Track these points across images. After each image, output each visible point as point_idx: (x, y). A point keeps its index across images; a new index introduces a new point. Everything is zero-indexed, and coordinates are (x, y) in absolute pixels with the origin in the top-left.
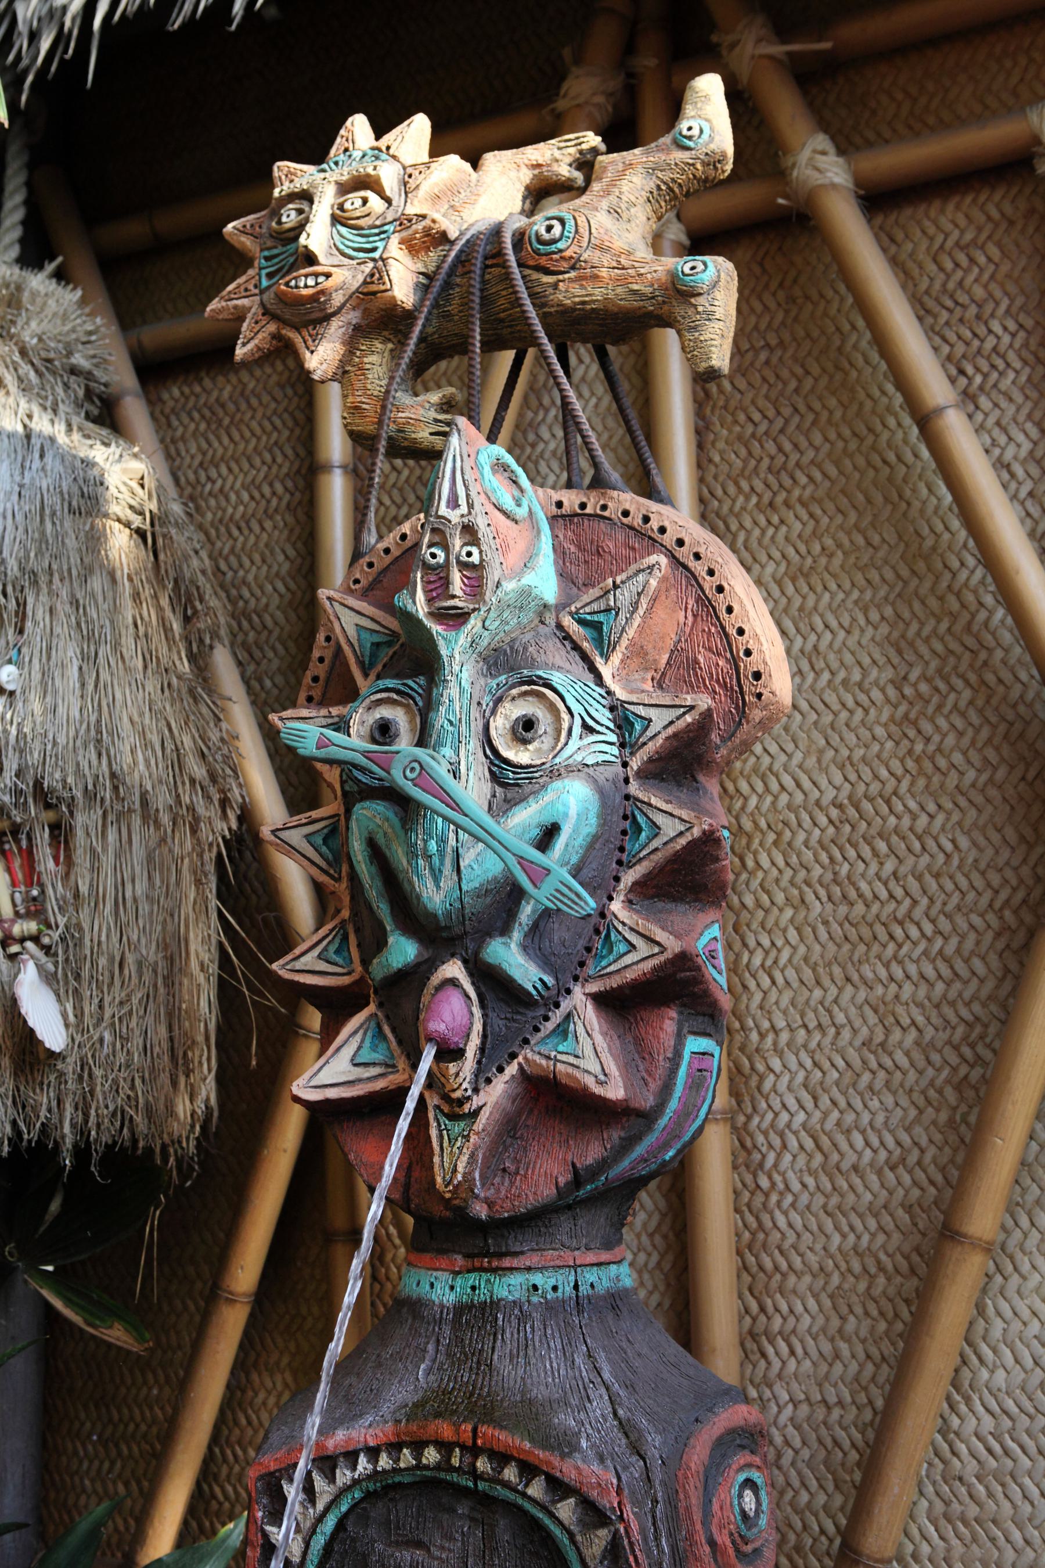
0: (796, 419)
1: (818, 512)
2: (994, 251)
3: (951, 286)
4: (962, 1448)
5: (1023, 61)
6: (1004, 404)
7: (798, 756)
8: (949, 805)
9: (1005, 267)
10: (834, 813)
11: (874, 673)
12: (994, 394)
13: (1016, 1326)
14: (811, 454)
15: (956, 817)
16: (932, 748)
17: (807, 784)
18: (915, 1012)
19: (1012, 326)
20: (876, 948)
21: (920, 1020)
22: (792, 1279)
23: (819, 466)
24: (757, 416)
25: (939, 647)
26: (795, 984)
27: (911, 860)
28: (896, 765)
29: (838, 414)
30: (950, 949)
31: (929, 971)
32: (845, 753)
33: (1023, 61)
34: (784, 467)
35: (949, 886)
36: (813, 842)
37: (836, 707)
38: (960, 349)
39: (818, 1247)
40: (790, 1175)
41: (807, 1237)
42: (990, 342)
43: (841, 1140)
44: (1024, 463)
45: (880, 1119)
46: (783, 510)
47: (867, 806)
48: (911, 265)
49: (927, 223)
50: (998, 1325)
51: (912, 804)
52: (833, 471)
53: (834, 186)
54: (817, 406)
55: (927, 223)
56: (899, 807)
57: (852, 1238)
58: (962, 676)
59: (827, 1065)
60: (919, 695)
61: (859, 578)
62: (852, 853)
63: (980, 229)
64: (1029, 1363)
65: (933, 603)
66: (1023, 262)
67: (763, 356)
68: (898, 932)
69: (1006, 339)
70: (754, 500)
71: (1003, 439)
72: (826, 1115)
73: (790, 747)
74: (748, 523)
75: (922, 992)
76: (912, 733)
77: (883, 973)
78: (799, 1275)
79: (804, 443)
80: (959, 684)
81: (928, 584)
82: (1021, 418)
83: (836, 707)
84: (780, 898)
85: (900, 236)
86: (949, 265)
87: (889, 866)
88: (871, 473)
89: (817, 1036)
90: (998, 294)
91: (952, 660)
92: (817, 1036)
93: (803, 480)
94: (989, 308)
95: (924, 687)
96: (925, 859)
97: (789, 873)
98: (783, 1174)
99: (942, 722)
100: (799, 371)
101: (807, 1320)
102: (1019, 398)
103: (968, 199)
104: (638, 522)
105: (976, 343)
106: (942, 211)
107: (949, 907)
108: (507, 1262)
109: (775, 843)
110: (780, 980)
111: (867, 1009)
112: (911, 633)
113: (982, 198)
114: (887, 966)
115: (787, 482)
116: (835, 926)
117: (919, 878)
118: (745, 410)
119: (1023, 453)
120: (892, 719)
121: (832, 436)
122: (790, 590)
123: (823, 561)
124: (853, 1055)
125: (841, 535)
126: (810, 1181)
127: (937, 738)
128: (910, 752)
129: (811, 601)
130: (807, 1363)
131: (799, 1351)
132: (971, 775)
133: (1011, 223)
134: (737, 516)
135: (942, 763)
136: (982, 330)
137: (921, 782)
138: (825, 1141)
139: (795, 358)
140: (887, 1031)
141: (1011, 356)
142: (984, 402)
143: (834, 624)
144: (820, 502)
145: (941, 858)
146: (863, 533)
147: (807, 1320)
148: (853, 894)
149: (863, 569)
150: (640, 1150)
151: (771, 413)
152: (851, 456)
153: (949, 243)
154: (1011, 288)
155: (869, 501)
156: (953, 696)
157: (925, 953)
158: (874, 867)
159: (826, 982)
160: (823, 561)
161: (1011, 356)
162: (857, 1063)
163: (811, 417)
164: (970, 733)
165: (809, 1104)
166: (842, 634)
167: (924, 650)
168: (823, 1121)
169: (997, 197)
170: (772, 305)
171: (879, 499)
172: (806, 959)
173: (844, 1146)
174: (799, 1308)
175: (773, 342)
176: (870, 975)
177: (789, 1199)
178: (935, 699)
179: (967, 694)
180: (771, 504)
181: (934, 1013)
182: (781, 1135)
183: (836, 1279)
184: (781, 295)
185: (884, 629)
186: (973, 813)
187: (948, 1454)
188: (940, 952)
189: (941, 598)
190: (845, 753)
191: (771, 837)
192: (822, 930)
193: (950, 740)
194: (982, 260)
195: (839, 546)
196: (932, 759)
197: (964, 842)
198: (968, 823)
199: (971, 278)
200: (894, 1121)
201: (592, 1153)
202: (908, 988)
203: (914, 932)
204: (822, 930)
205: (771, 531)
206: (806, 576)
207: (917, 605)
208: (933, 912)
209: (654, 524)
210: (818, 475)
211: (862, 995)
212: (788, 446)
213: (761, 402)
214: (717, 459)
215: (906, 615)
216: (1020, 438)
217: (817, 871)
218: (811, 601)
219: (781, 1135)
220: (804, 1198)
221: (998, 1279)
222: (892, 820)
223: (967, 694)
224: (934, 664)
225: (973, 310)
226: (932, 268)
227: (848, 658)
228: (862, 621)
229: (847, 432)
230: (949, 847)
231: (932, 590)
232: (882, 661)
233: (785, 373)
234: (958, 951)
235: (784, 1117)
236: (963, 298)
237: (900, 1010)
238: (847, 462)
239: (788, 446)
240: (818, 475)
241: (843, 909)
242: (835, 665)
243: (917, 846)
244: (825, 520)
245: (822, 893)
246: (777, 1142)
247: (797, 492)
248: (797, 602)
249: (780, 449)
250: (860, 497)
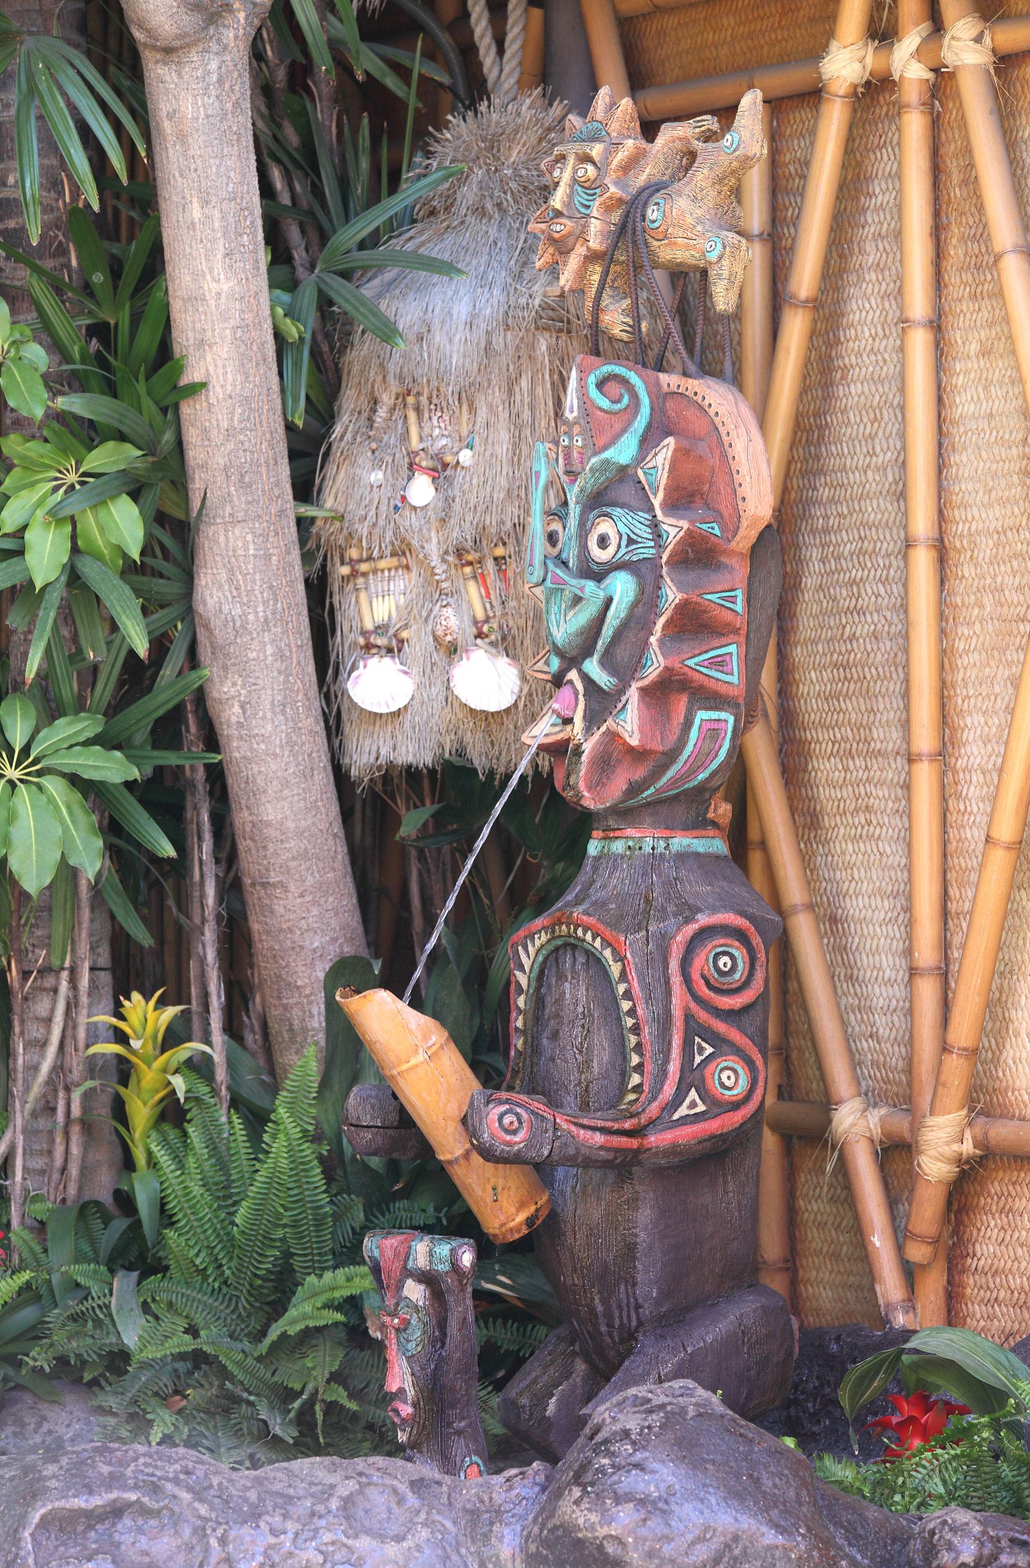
104: (700, 400)
108: (617, 834)
148: (1003, 600)
150: (670, 773)
168: (987, 762)
201: (639, 773)
209: (706, 402)
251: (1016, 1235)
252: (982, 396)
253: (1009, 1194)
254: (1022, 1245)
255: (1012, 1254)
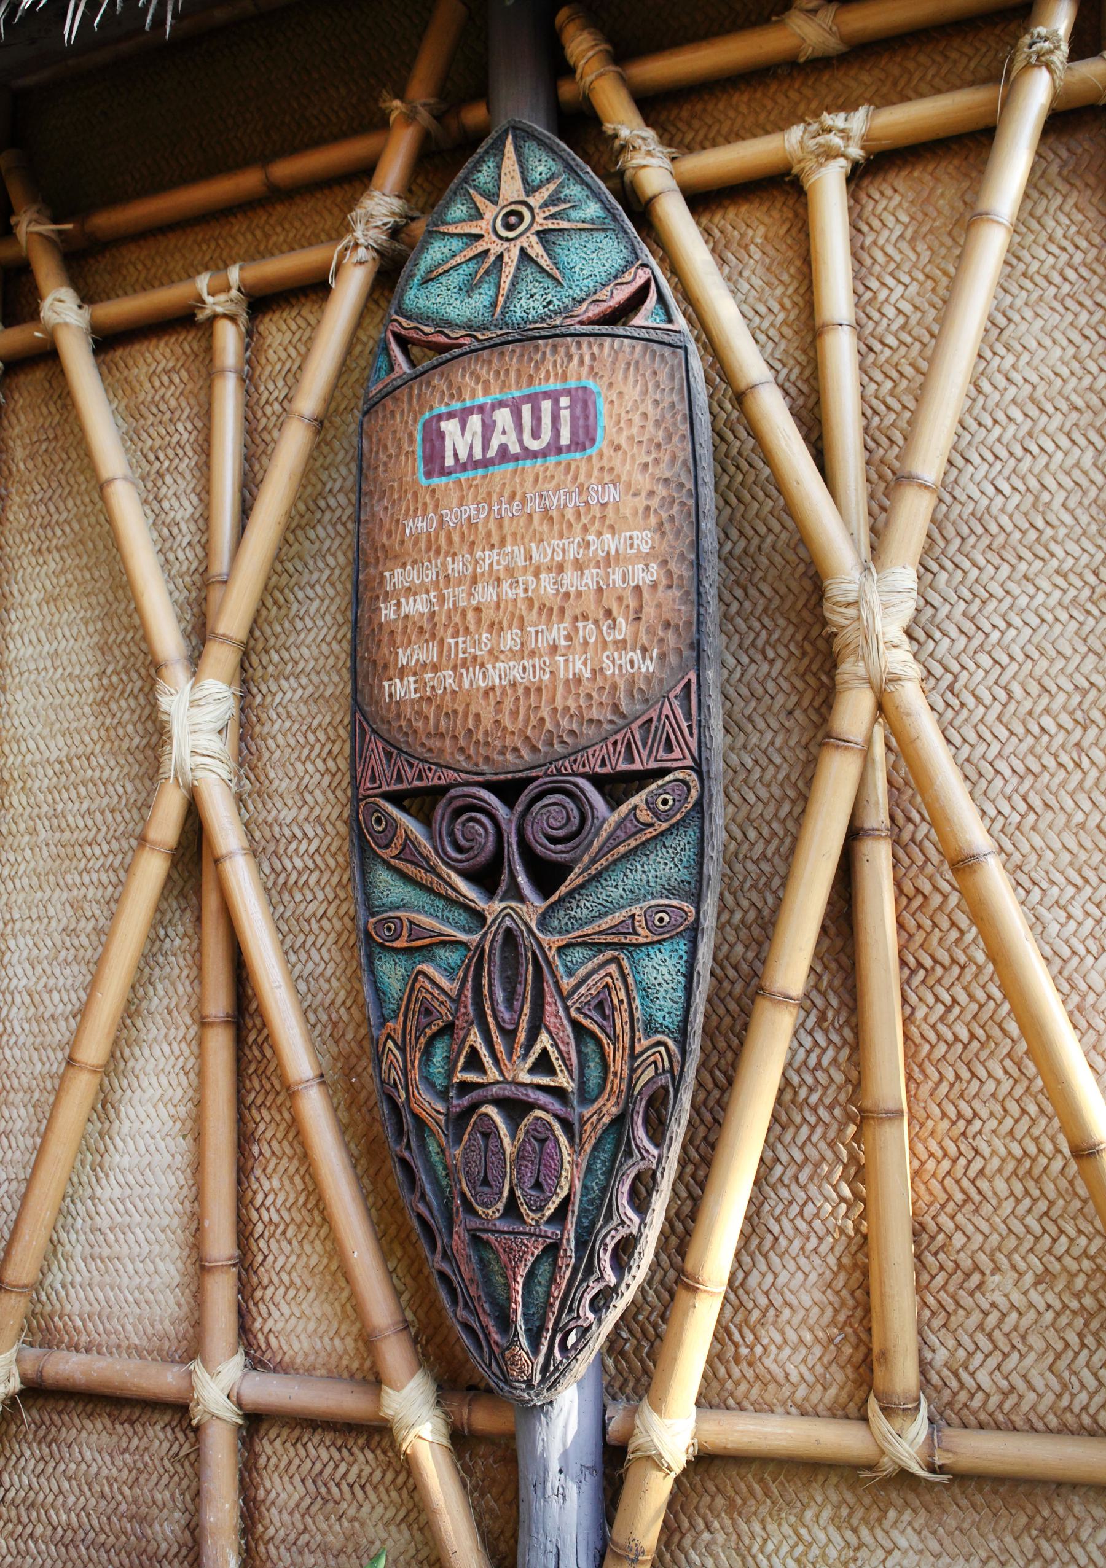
0: (60, 490)
1: (65, 555)
2: (184, 374)
3: (157, 398)
4: (102, 1209)
5: (213, 245)
6: (180, 481)
7: (39, 727)
8: (123, 762)
9: (190, 386)
10: (57, 767)
11: (88, 667)
12: (175, 474)
13: (137, 1124)
14: (65, 515)
15: (126, 770)
16: (116, 721)
17: (42, 747)
18: (95, 906)
19: (190, 427)
20: (75, 861)
21: (97, 912)
22: (12, 1094)
23: (69, 524)
24: (37, 488)
25: (126, 650)
26: (27, 888)
27: (98, 800)
28: (94, 733)
29: (83, 487)
30: (116, 864)
31: (105, 880)
32: (66, 725)
33: (213, 245)
34: (49, 524)
35: (119, 819)
36: (44, 789)
37: (64, 692)
38: (158, 442)
39: (28, 1072)
40: (16, 1023)
41: (22, 1064)
42: (176, 437)
43: (45, 996)
44: (187, 521)
45: (69, 982)
46: (46, 553)
47: (76, 762)
48: (135, 383)
49: (147, 355)
50: (127, 1123)
51: (102, 761)
52: (76, 527)
53: (66, 324)
54: (72, 481)
55: (147, 355)
56: (94, 763)
57: (48, 1065)
58: (137, 671)
59: (41, 945)
60: (111, 684)
61: (85, 602)
62: (65, 795)
63: (178, 360)
64: (143, 1150)
65: (125, 619)
66: (201, 383)
67: (44, 446)
68: (88, 851)
69: (186, 435)
70: (30, 547)
71: (176, 505)
72: (39, 979)
73: (35, 721)
74: (25, 564)
75: (99, 894)
76: (105, 711)
77: (78, 880)
78: (16, 1091)
79: (62, 507)
80: (134, 676)
81: (123, 606)
82: (189, 491)
83: (64, 692)
84: (22, 827)
85: (131, 363)
86: (157, 384)
87: (85, 806)
88: (98, 528)
89: (37, 924)
90: (184, 404)
91: (132, 659)
92: (37, 924)
93: (59, 533)
94: (177, 414)
95: (115, 679)
96: (106, 800)
97: (29, 809)
98: (11, 1022)
99: (123, 703)
100: (64, 456)
101: (19, 1123)
102: (189, 477)
103: (173, 340)
105: (168, 438)
106: (157, 347)
107: (118, 834)
109: (22, 788)
110: (18, 886)
111: (67, 905)
112: (110, 641)
113: (181, 338)
114: (80, 874)
115: (50, 534)
116: (52, 847)
117: (102, 813)
118: (30, 483)
119: (188, 515)
120: (94, 701)
121: (79, 502)
122: (45, 609)
123: (65, 590)
124: (57, 938)
125: (77, 572)
126: (26, 1026)
127: (119, 714)
128: (103, 724)
129: (56, 619)
130: (18, 1153)
131: (14, 1145)
132: (137, 740)
133: (197, 356)
134: (19, 558)
135: (121, 732)
136: (171, 429)
137: (108, 745)
138: (36, 998)
139: (63, 448)
140: (78, 921)
141: (188, 448)
142: (168, 479)
143: (68, 634)
144: (67, 548)
145: (116, 798)
146: (89, 569)
147: (19, 1123)
148: (64, 825)
149: (87, 595)
151: (45, 486)
152: (87, 516)
153: (159, 369)
154: (192, 401)
155: (95, 548)
156: (130, 685)
157: (103, 866)
158: (77, 804)
159: (45, 886)
160: (65, 590)
161: (188, 448)
162: (59, 944)
163: (67, 489)
164: (138, 711)
165: (29, 972)
166: (72, 641)
167: (117, 652)
168: (36, 983)
169: (190, 338)
170: (53, 410)
171: (101, 546)
172: (34, 871)
173: (47, 1002)
174: (15, 1115)
175: (51, 436)
176: (70, 882)
177: (14, 1039)
178: (120, 687)
179: (139, 683)
180: (39, 550)
181: (106, 908)
182: (12, 994)
183: (37, 1095)
184: (59, 403)
185: (96, 638)
186: (137, 767)
187: (93, 1214)
188: (111, 865)
189: (130, 616)
190: (66, 725)
191: (20, 784)
192: (45, 849)
193: (127, 716)
194: (177, 380)
195: (75, 579)
196: (115, 729)
197: (129, 788)
198: (133, 774)
199: (169, 393)
200: (77, 984)
202: (92, 890)
203: (97, 851)
204: (45, 849)
205: (38, 569)
206: (55, 600)
207: (116, 621)
208: (109, 837)
210: (67, 529)
211: (65, 895)
212: (52, 509)
213: (42, 479)
214: (11, 518)
215: (109, 628)
216: (186, 504)
217: (45, 808)
218: (56, 619)
219: (12, 994)
220: (22, 1039)
221: (129, 1092)
222: (90, 772)
223: (139, 683)
224: (121, 663)
225: (168, 415)
226: (147, 385)
227: (74, 658)
228: (84, 632)
229: (87, 500)
230: (120, 790)
231: (125, 610)
232: (92, 660)
233: (56, 458)
234: (121, 864)
235: (15, 981)
236: (163, 407)
237: (86, 906)
238: (85, 521)
239: (52, 509)
240: (67, 529)
241: (58, 835)
242: (66, 663)
243: (102, 790)
244: (69, 561)
245: (47, 823)
246: (9, 999)
247: (54, 542)
248: (48, 619)
249: (48, 512)
250: (90, 545)
251: (62, 1467)
252: (44, 639)
253: (53, 1423)
254: (69, 1479)
255: (55, 1488)
